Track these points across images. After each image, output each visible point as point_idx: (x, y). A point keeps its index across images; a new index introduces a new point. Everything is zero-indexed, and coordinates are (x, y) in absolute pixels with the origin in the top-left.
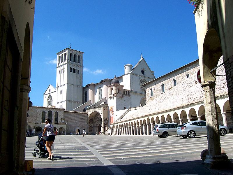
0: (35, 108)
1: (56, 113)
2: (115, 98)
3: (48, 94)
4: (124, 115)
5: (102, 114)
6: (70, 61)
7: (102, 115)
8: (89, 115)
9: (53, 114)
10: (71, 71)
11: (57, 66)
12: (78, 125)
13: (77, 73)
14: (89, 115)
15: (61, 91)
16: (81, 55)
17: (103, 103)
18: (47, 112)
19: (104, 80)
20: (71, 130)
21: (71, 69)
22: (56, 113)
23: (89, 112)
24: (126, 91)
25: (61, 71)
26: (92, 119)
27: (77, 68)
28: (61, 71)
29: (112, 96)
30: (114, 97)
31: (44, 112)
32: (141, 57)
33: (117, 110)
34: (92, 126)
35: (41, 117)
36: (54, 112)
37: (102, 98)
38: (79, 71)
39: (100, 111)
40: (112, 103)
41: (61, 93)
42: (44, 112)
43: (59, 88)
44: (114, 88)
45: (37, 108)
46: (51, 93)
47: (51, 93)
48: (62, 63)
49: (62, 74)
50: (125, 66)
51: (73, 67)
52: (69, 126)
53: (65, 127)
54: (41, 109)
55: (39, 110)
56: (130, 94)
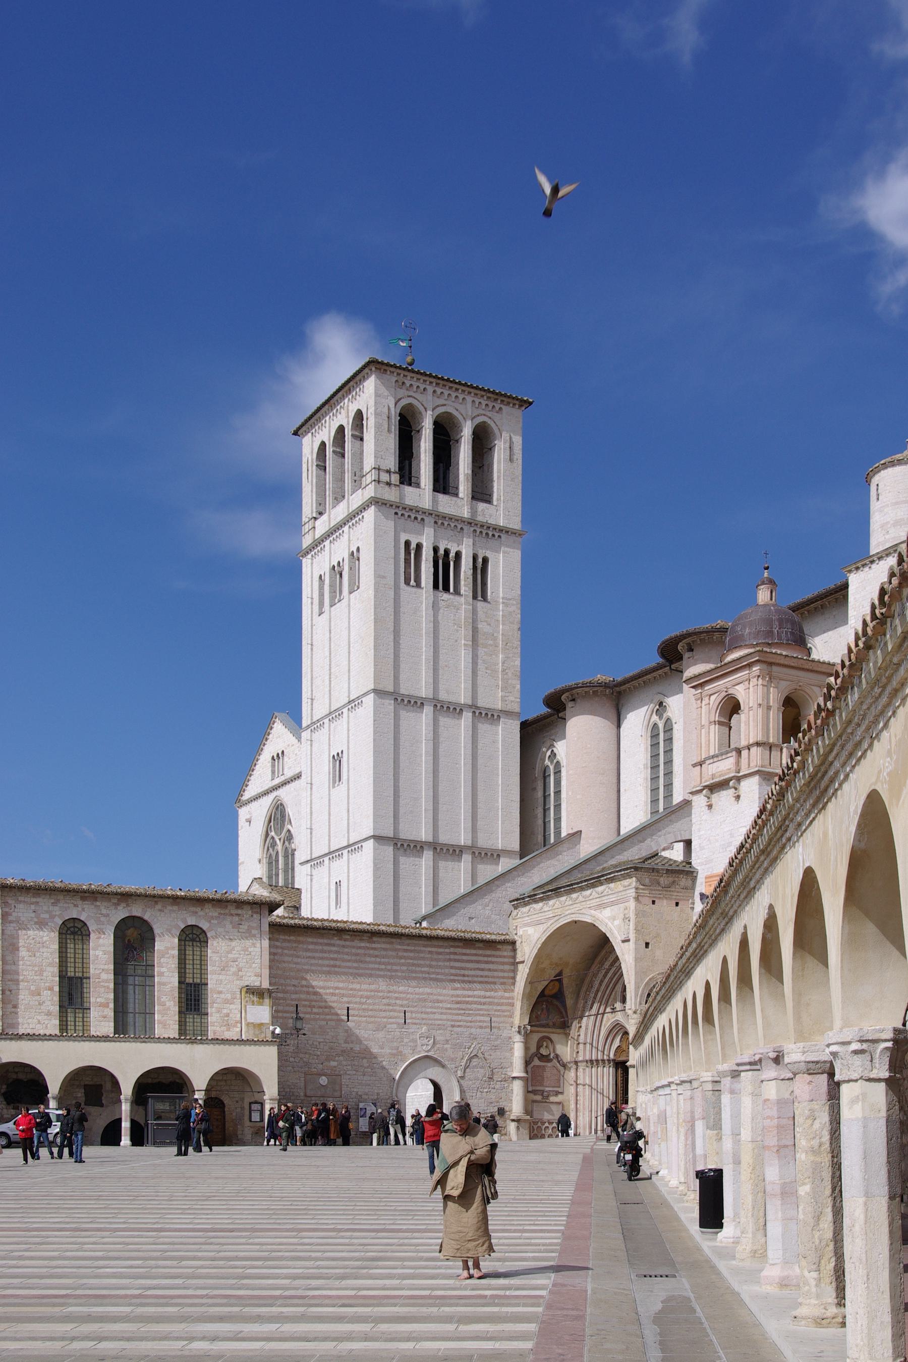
1: (192, 938)
3: (266, 793)
8: (527, 951)
10: (411, 578)
11: (307, 541)
14: (527, 951)
15: (337, 759)
19: (689, 635)
23: (531, 930)
25: (332, 586)
26: (559, 996)
28: (339, 579)
29: (724, 767)
41: (337, 776)
43: (321, 736)
46: (284, 784)
47: (284, 784)
48: (339, 512)
49: (341, 607)
54: (45, 903)
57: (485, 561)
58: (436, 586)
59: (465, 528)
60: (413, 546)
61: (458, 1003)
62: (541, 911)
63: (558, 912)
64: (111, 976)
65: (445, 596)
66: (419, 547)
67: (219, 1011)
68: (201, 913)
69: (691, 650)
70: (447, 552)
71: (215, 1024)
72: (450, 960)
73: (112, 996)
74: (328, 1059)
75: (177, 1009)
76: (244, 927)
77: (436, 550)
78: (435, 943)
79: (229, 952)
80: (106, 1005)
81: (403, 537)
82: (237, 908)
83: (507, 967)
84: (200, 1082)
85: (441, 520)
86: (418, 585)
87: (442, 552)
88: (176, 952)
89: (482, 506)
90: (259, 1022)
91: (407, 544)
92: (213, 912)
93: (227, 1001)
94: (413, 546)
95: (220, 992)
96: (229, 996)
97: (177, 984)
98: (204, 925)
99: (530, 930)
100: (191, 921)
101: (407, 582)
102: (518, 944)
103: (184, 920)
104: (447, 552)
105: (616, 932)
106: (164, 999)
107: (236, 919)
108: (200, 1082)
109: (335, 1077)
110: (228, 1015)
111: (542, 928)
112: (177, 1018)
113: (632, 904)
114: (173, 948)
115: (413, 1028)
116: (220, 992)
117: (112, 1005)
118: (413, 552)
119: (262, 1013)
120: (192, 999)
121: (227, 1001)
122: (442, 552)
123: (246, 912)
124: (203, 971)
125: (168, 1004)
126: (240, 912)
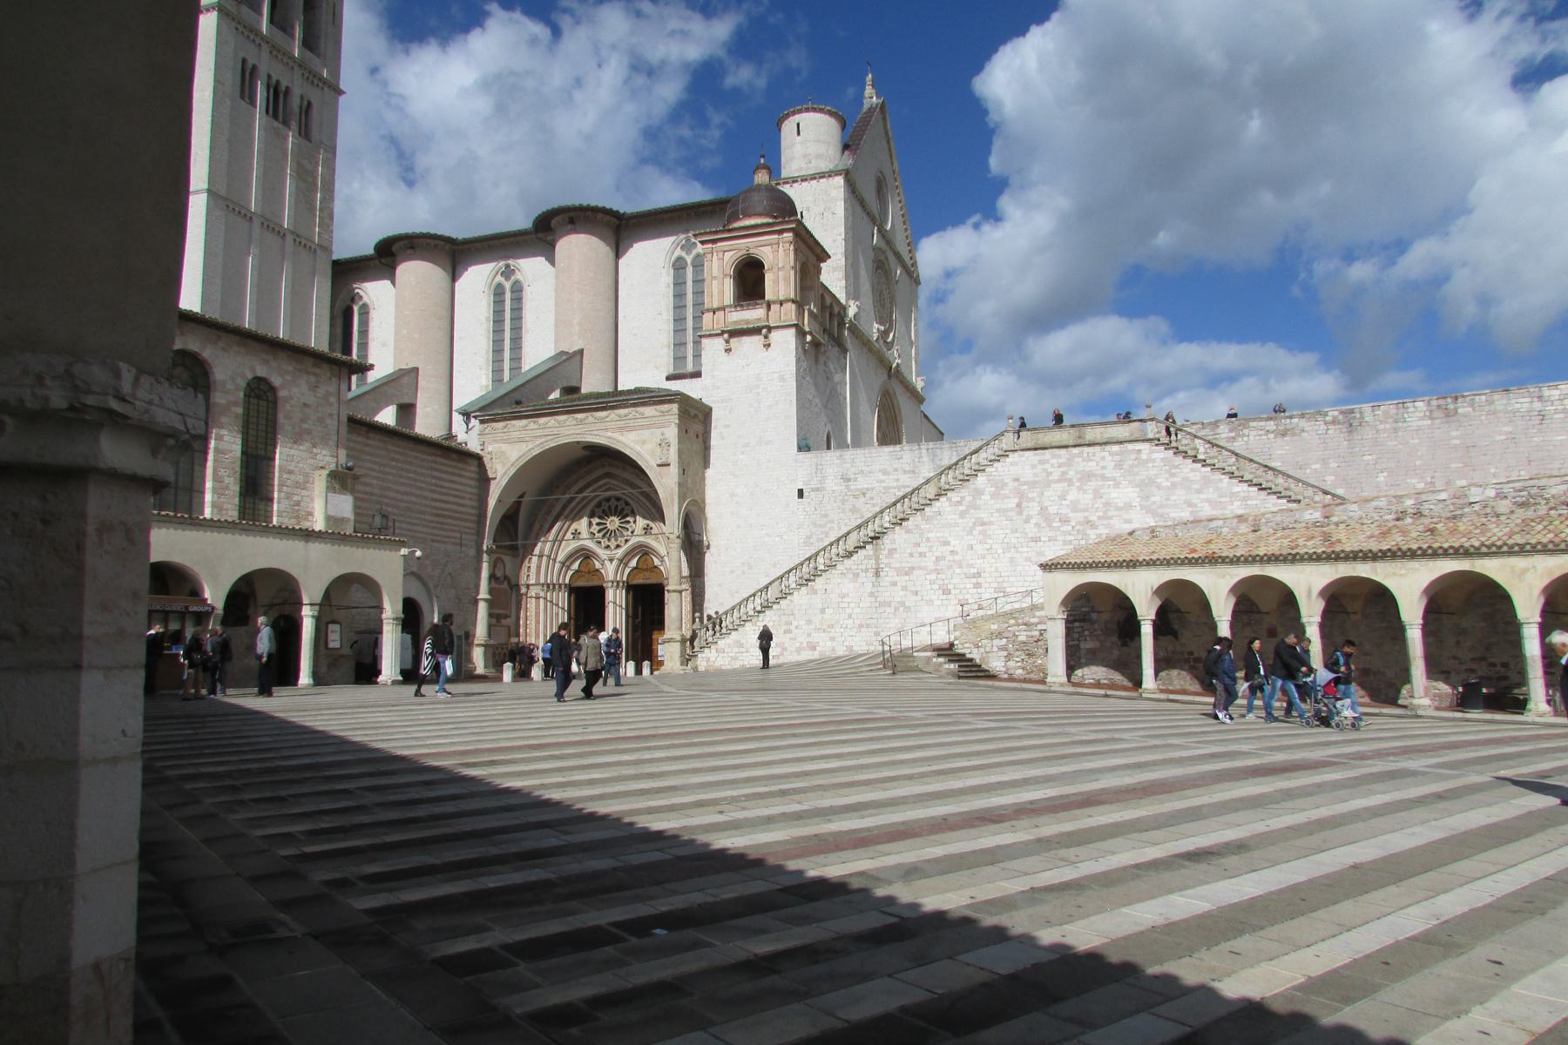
1: (261, 395)
2: (785, 342)
4: (930, 491)
5: (674, 470)
7: (666, 484)
10: (247, 93)
17: (555, 395)
21: (247, 75)
22: (261, 395)
23: (508, 451)
24: (831, 306)
30: (770, 329)
32: (869, 90)
33: (804, 447)
34: (506, 578)
37: (538, 350)
38: (307, 109)
39: (647, 441)
40: (755, 381)
44: (777, 256)
50: (800, 111)
53: (387, 567)
57: (309, 104)
60: (249, 66)
61: (437, 515)
62: (524, 428)
63: (555, 431)
65: (276, 124)
66: (254, 68)
67: (289, 496)
68: (273, 364)
69: (572, 221)
71: (278, 513)
72: (432, 469)
75: (237, 488)
76: (321, 391)
77: (269, 76)
78: (422, 448)
79: (303, 420)
81: (242, 55)
82: (315, 365)
83: (473, 483)
86: (253, 103)
88: (240, 410)
89: (309, 54)
90: (340, 515)
91: (244, 61)
93: (297, 485)
94: (249, 66)
95: (291, 472)
96: (301, 478)
97: (239, 454)
98: (276, 381)
99: (504, 447)
100: (261, 372)
101: (242, 97)
102: (486, 460)
103: (253, 369)
105: (648, 457)
106: (222, 472)
107: (313, 379)
110: (298, 503)
111: (524, 447)
112: (237, 500)
113: (672, 433)
114: (235, 404)
116: (291, 472)
119: (345, 505)
125: (227, 480)
126: (317, 371)
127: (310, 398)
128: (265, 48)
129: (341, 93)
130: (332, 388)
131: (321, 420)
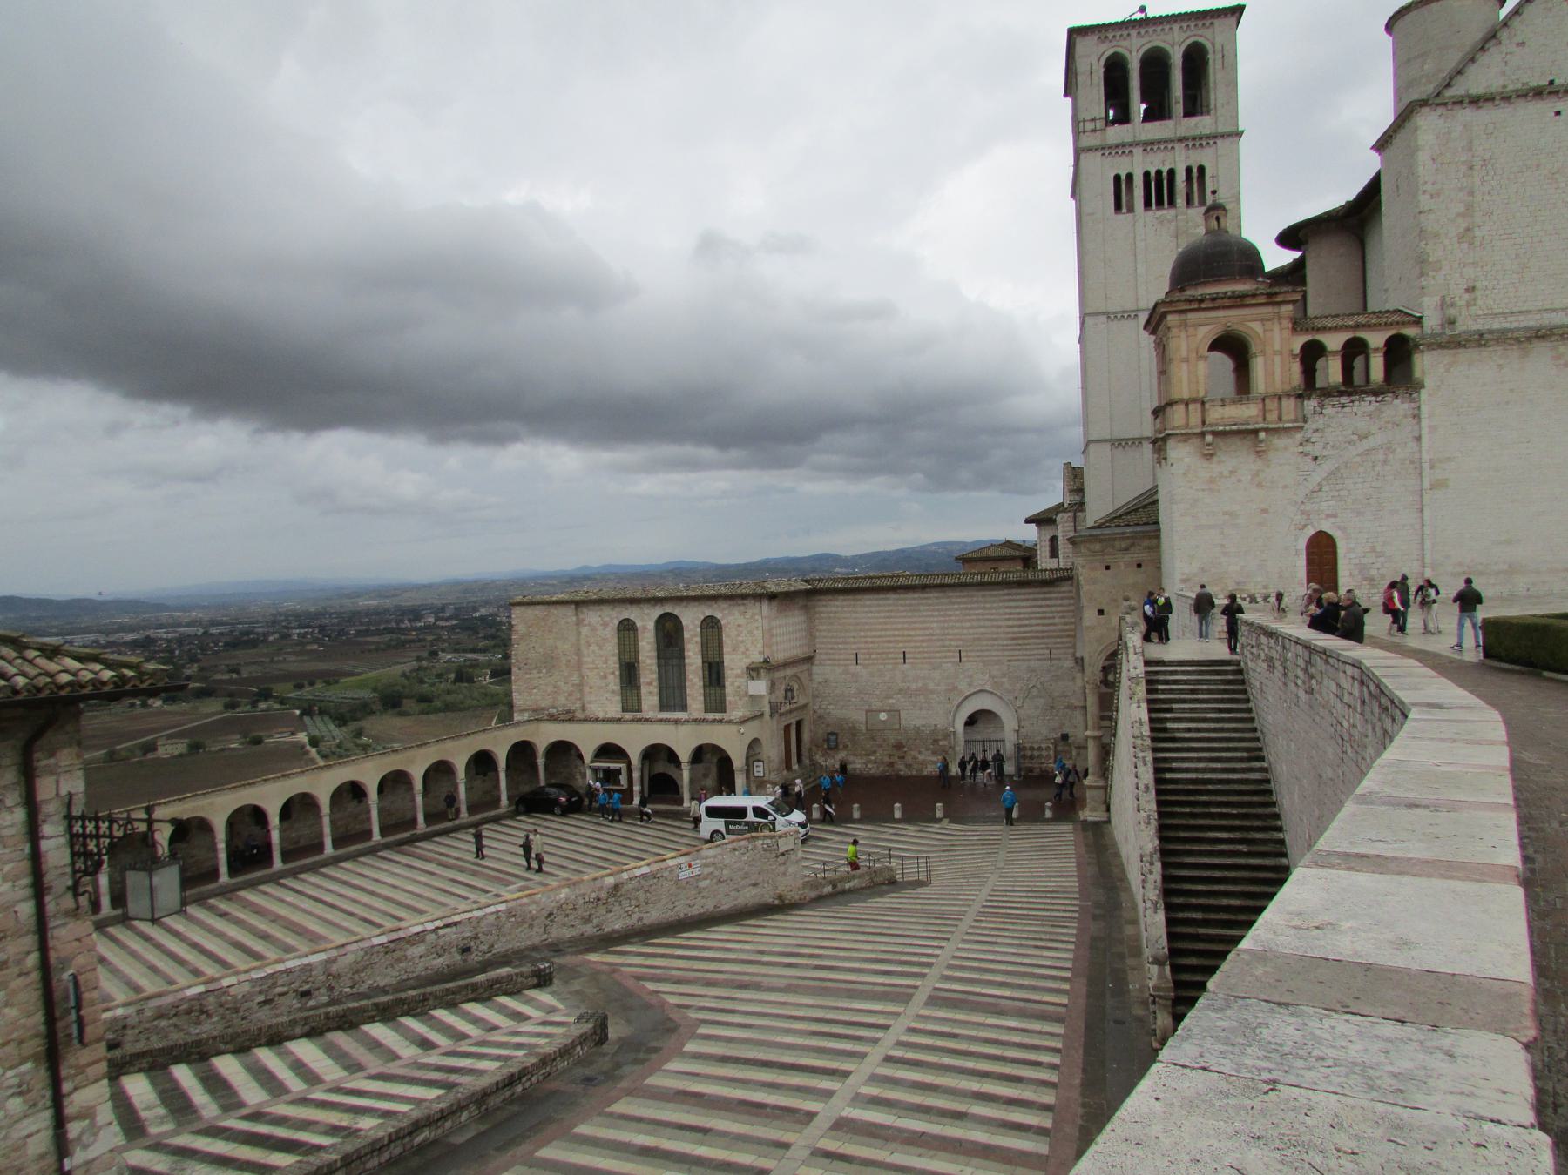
0: (561, 610)
1: (711, 626)
6: (1100, 124)
9: (686, 635)
12: (982, 681)
13: (1180, 200)
16: (1208, 36)
18: (646, 620)
20: (919, 723)
22: (711, 626)
27: (1179, 161)
31: (627, 627)
35: (613, 664)
36: (691, 618)
38: (1197, 175)
42: (627, 627)
45: (569, 611)
51: (1139, 165)
52: (900, 691)
55: (593, 616)
56: (1425, 364)
57: (1201, 169)
58: (1147, 204)
59: (1177, 146)
64: (655, 661)
65: (1159, 213)
66: (1130, 177)
70: (1159, 173)
73: (655, 676)
74: (888, 697)
76: (748, 615)
80: (650, 684)
84: (684, 755)
85: (1148, 145)
87: (1153, 174)
92: (723, 604)
98: (719, 616)
104: (1159, 173)
108: (684, 755)
109: (894, 712)
115: (968, 665)
117: (656, 683)
118: (1121, 185)
120: (714, 674)
121: (738, 676)
122: (1153, 174)
123: (750, 603)
124: (721, 654)
127: (741, 621)
128: (1138, 151)
129: (1239, 134)
130: (756, 610)
131: (750, 633)
